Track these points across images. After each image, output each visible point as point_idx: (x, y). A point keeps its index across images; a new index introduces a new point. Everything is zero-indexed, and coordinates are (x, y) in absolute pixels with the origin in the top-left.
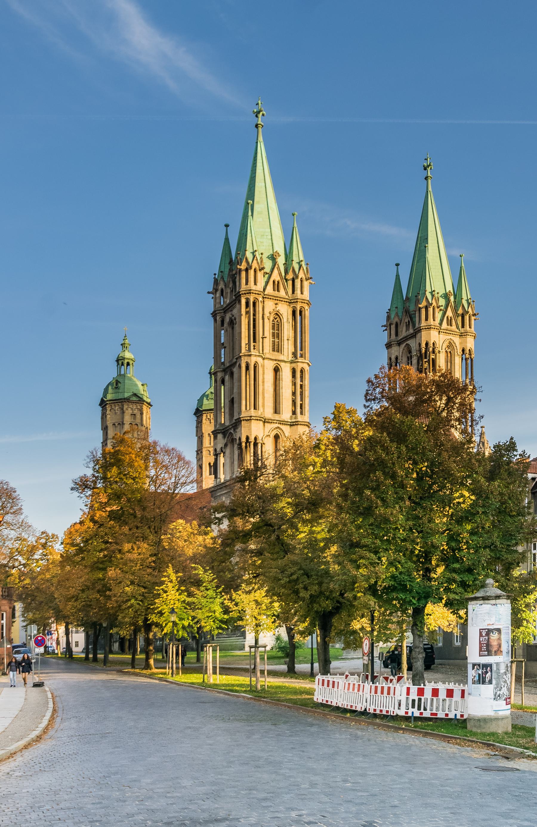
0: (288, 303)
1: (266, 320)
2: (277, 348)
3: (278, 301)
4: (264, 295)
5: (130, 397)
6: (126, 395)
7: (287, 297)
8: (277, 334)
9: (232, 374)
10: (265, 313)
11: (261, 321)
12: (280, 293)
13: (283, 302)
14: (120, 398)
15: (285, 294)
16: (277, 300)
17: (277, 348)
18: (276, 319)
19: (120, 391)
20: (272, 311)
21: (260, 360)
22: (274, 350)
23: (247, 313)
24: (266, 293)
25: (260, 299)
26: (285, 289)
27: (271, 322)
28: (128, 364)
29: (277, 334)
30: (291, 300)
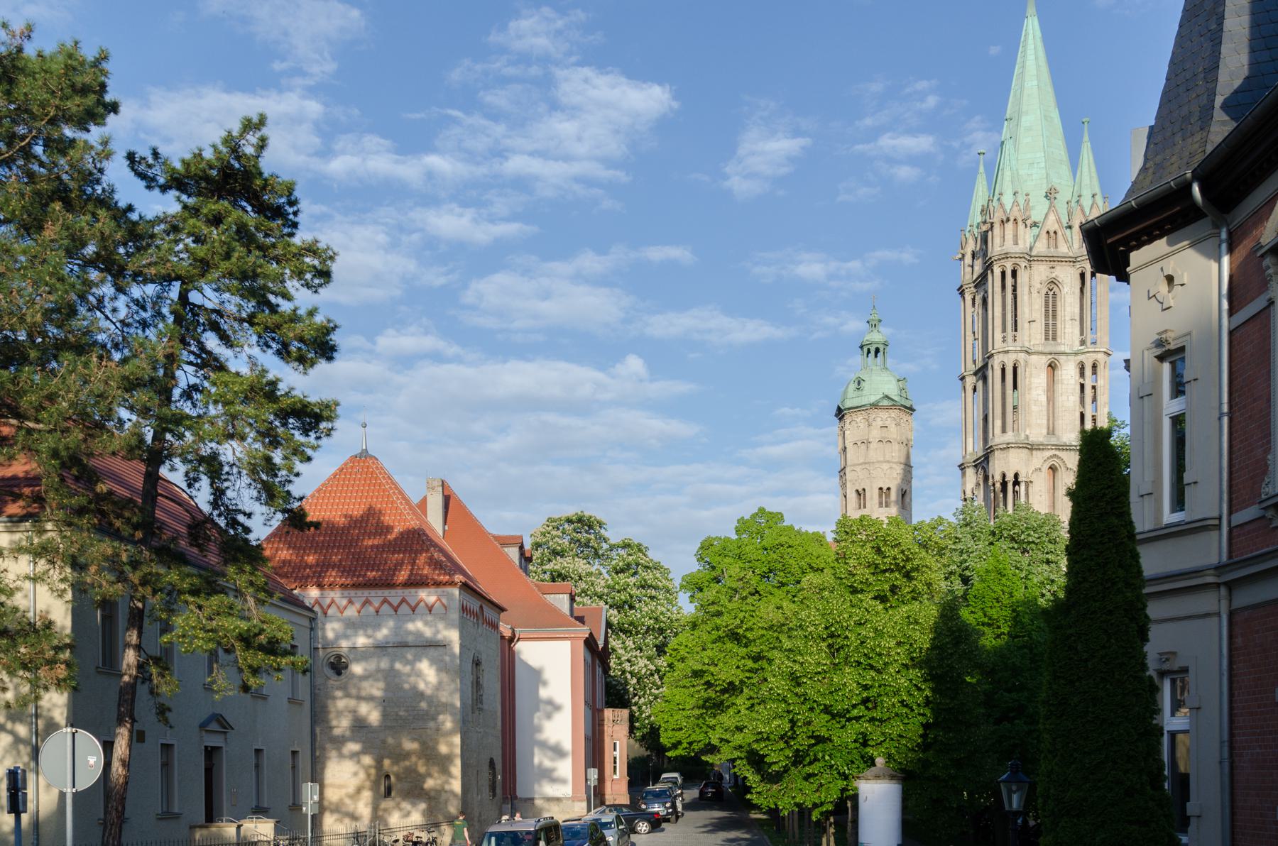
0: (1072, 264)
1: (1035, 295)
2: (1051, 334)
3: (1056, 263)
4: (1031, 256)
5: (878, 402)
6: (873, 399)
7: (1071, 254)
8: (1051, 311)
9: (985, 379)
10: (1032, 283)
11: (1026, 297)
12: (1059, 250)
13: (1064, 263)
14: (863, 403)
15: (1066, 250)
16: (1053, 260)
17: (1051, 334)
18: (1051, 290)
19: (864, 392)
20: (1045, 278)
21: (1022, 355)
22: (1047, 339)
23: (1004, 287)
24: (1033, 254)
25: (1023, 263)
26: (1067, 241)
27: (1044, 296)
28: (877, 351)
29: (1051, 311)
30: (1076, 258)
